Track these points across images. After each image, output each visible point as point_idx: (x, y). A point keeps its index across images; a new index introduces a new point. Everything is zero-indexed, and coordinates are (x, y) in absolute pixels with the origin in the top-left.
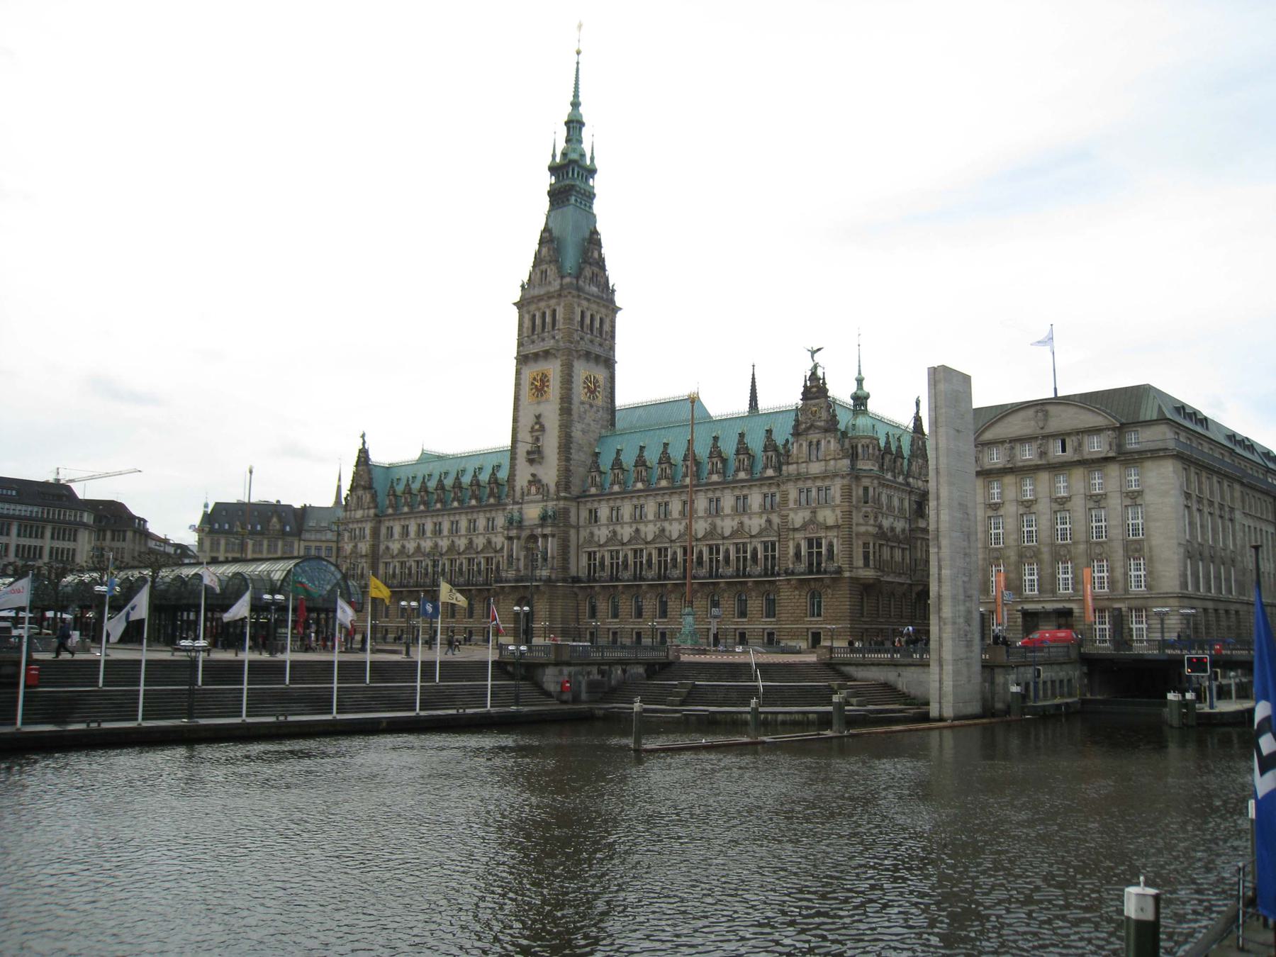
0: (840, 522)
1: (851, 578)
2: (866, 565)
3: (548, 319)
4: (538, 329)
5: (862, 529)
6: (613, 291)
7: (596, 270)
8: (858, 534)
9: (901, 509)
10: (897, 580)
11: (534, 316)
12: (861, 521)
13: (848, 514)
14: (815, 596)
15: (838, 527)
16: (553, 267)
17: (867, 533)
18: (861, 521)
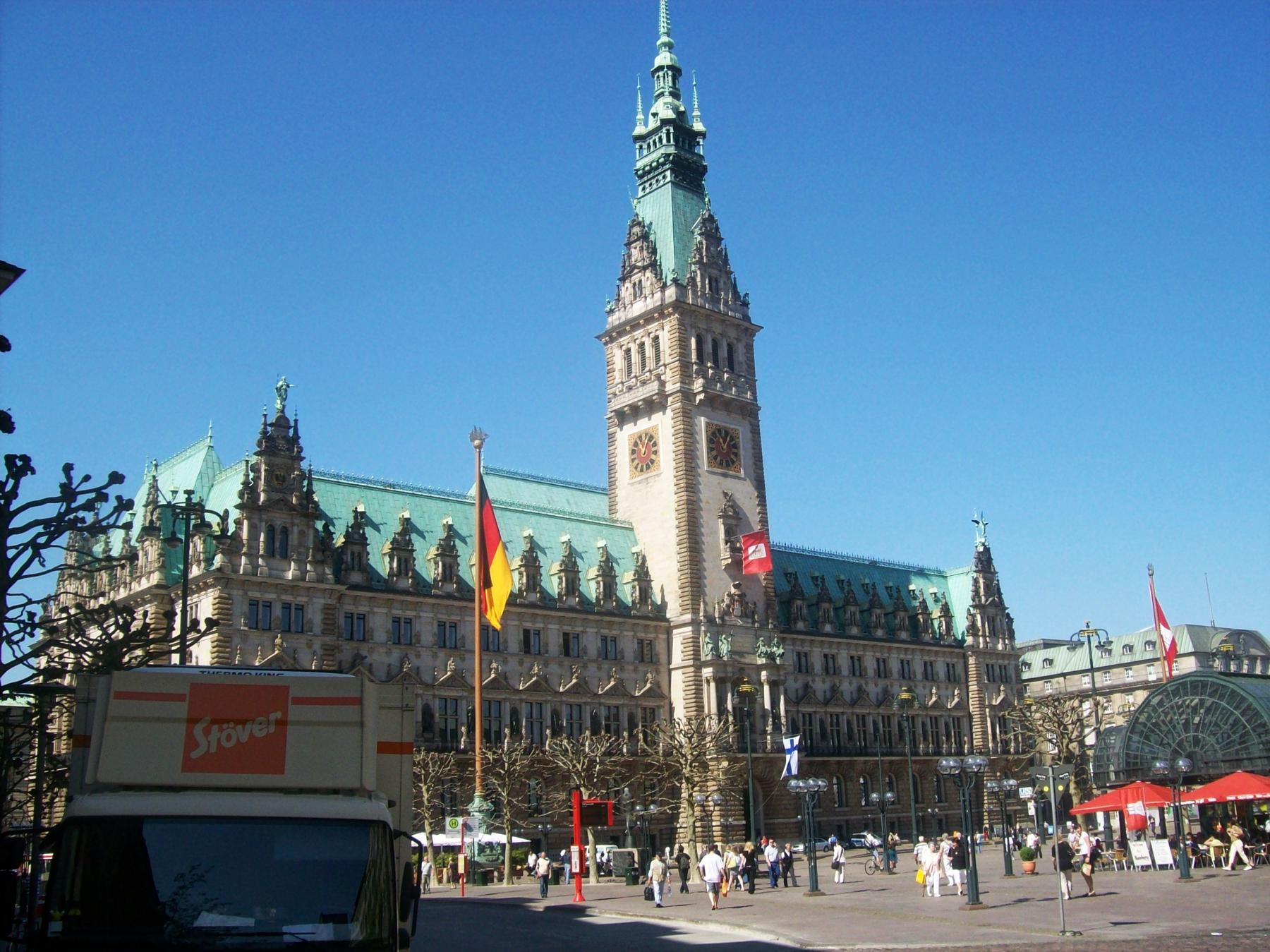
3: (649, 351)
4: (636, 370)
6: (745, 304)
7: (714, 272)
11: (628, 351)
16: (648, 273)
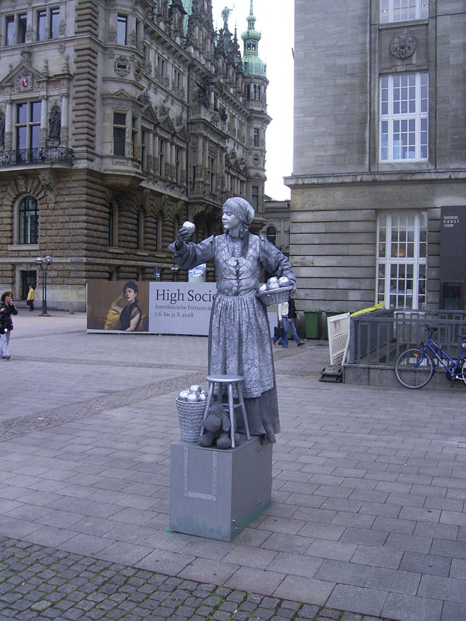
0: (73, 69)
1: (90, 172)
2: (119, 151)
5: (113, 88)
8: (105, 97)
9: (177, 86)
10: (168, 192)
12: (113, 74)
13: (88, 57)
14: (27, 205)
15: (68, 77)
17: (120, 96)
18: (113, 74)
